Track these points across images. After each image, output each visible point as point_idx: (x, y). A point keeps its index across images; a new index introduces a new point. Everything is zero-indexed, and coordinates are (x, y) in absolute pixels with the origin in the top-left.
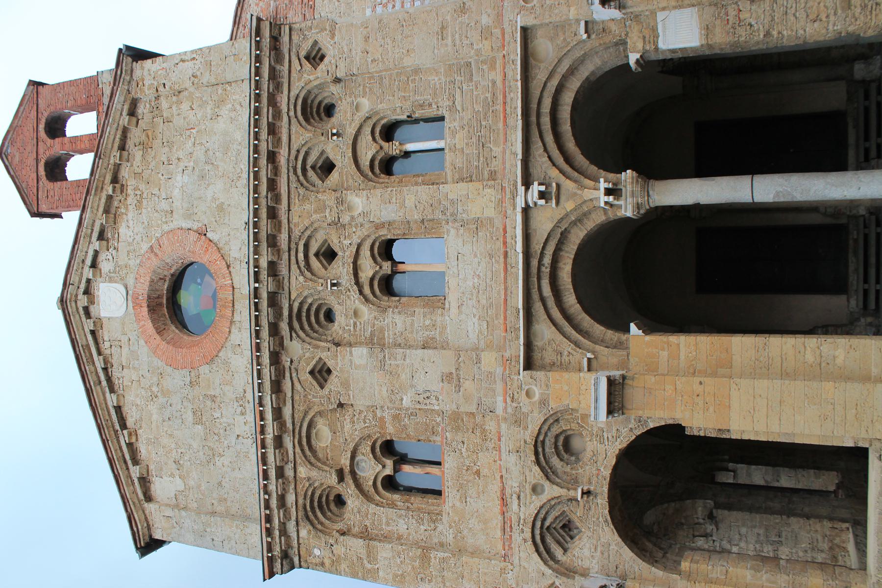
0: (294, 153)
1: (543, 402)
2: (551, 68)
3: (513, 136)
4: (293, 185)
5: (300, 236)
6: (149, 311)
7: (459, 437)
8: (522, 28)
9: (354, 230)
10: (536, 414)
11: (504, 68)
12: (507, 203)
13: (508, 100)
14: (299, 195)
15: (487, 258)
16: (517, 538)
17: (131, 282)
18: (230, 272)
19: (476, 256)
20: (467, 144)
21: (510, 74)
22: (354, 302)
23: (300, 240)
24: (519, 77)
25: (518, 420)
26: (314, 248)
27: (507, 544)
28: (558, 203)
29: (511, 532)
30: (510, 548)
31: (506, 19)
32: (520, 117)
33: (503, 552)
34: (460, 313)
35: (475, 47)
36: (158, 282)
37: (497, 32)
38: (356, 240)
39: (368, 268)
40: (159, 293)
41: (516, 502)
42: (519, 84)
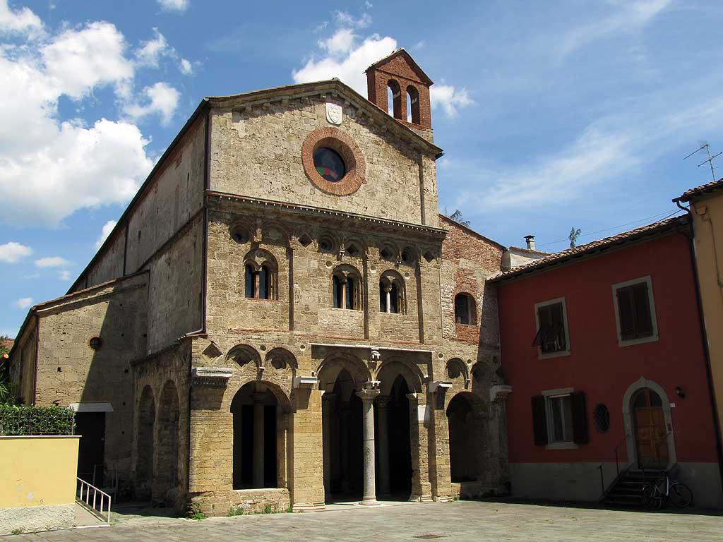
0: (395, 241)
1: (300, 353)
6: (329, 137)
7: (279, 310)
10: (294, 349)
12: (372, 342)
16: (241, 337)
25: (291, 341)
31: (434, 346)
33: (233, 329)
41: (256, 337)
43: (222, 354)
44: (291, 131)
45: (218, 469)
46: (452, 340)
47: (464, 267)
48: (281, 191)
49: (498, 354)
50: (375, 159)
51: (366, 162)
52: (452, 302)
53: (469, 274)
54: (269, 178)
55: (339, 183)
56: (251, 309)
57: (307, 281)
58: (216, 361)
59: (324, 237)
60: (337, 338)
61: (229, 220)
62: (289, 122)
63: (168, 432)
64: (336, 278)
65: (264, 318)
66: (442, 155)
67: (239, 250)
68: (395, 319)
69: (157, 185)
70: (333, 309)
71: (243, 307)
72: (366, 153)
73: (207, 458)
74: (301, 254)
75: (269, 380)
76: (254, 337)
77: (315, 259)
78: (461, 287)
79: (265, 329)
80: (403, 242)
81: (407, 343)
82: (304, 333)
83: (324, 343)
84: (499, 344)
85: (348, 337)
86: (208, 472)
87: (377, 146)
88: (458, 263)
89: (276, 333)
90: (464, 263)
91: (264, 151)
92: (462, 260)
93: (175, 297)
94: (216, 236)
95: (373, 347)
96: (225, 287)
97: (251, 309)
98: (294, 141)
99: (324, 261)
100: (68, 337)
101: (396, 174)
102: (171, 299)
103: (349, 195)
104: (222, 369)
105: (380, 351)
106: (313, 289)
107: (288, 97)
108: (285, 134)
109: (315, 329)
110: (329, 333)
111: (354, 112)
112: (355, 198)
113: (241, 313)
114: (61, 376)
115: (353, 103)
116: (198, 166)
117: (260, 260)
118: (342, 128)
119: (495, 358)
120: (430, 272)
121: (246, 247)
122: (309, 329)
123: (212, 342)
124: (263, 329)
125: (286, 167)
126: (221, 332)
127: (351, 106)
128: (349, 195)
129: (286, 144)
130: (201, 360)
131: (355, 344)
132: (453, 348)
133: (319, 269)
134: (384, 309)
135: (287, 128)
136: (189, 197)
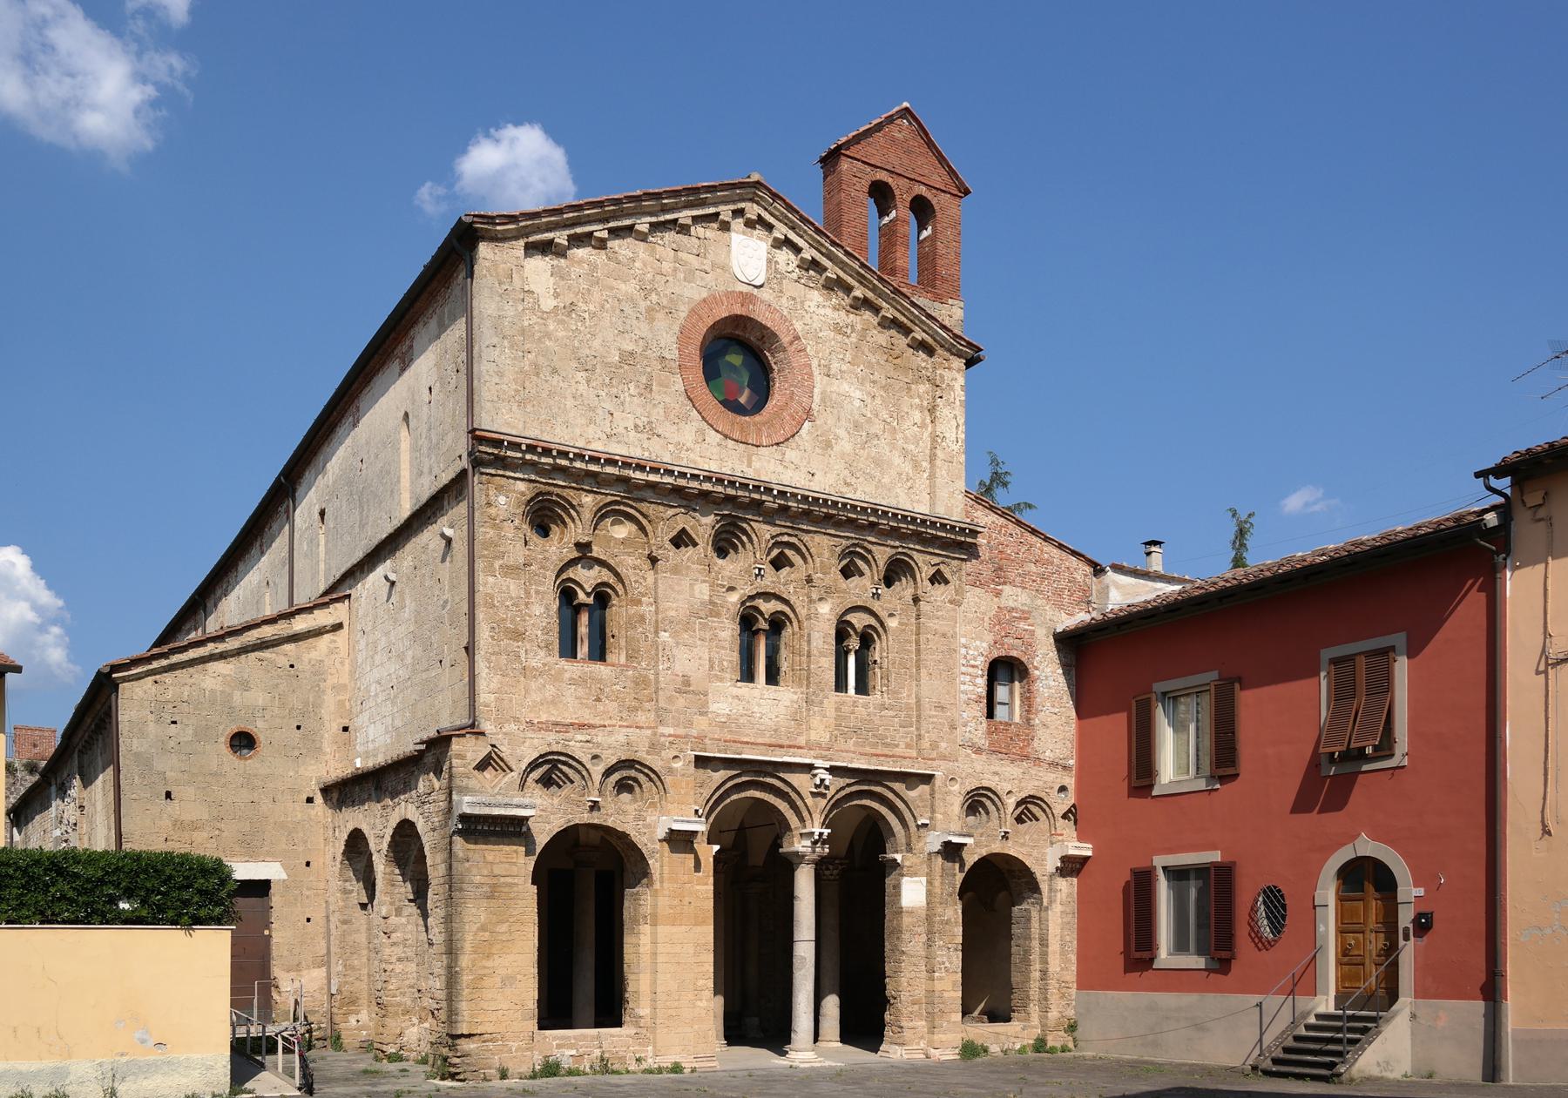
2: (901, 794)
3: (863, 761)
4: (845, 542)
5: (802, 541)
7: (629, 684)
8: (934, 775)
9: (801, 598)
11: (910, 758)
13: (888, 759)
14: (836, 546)
15: (774, 727)
16: (551, 737)
17: (765, 294)
18: (772, 446)
19: (777, 717)
20: (857, 718)
21: (905, 762)
22: (742, 589)
23: (799, 540)
24: (903, 770)
26: (789, 553)
27: (544, 726)
28: (812, 793)
29: (556, 731)
30: (540, 729)
31: (941, 762)
32: (876, 768)
34: (733, 697)
35: (927, 735)
36: (762, 333)
37: (934, 755)
38: (793, 599)
39: (769, 607)
40: (749, 330)
41: (584, 739)
42: (898, 769)
43: (512, 771)
44: (654, 297)
45: (508, 991)
46: (979, 751)
47: (1011, 604)
48: (632, 433)
49: (1070, 782)
50: (835, 366)
51: (816, 373)
52: (982, 676)
53: (1020, 618)
54: (608, 406)
55: (757, 418)
56: (573, 682)
57: (688, 627)
58: (502, 784)
59: (724, 536)
60: (747, 743)
61: (523, 494)
62: (649, 276)
63: (404, 920)
64: (747, 621)
65: (598, 700)
66: (979, 360)
67: (545, 558)
68: (866, 706)
69: (358, 408)
70: (739, 684)
71: (557, 678)
72: (817, 352)
73: (486, 971)
74: (676, 570)
75: (609, 823)
76: (579, 737)
77: (705, 581)
78: (1003, 644)
79: (602, 723)
80: (888, 549)
81: (886, 756)
82: (681, 731)
83: (719, 752)
84: (1072, 762)
85: (767, 741)
86: (490, 996)
87: (839, 337)
88: (998, 594)
89: (624, 730)
90: (1013, 596)
91: (596, 343)
92: (1007, 589)
93: (410, 653)
94: (494, 526)
95: (818, 763)
96: (518, 635)
97: (573, 682)
98: (661, 322)
99: (724, 586)
100: (183, 730)
101: (878, 401)
102: (401, 657)
103: (777, 444)
104: (516, 801)
105: (833, 770)
106: (699, 642)
107: (649, 219)
108: (643, 305)
109: (701, 724)
110: (730, 732)
111: (792, 257)
112: (791, 454)
113: (550, 690)
114: (173, 808)
115: (792, 236)
116: (451, 372)
117: (588, 578)
118: (765, 294)
119: (1063, 789)
120: (940, 613)
121: (558, 547)
122: (690, 724)
123: (493, 746)
124: (597, 721)
125: (644, 380)
126: (513, 727)
127: (787, 243)
128: (777, 444)
129: (643, 329)
130: (472, 783)
131: (782, 756)
132: (979, 768)
133: (711, 602)
134: (841, 685)
135: (646, 292)
136: (434, 441)
